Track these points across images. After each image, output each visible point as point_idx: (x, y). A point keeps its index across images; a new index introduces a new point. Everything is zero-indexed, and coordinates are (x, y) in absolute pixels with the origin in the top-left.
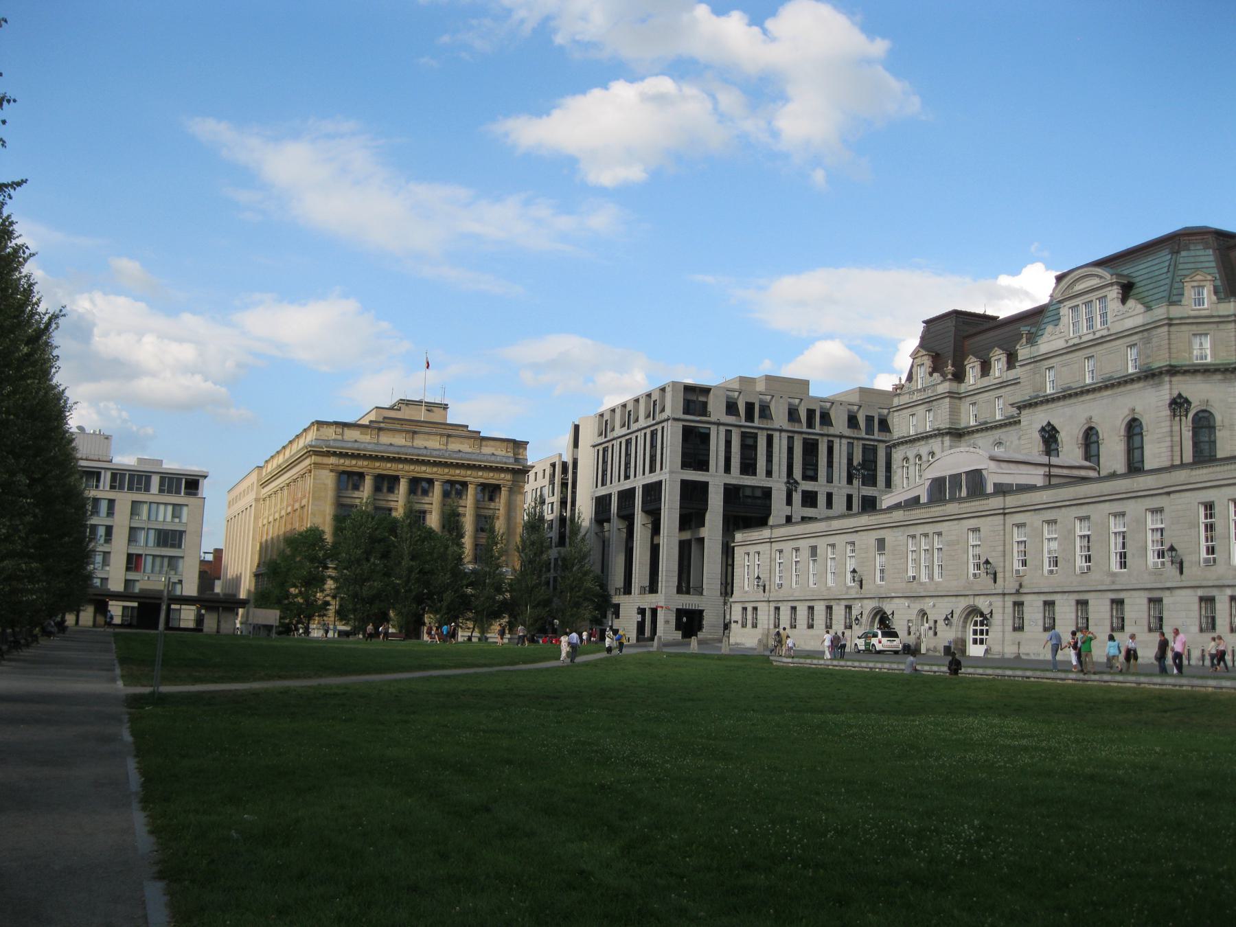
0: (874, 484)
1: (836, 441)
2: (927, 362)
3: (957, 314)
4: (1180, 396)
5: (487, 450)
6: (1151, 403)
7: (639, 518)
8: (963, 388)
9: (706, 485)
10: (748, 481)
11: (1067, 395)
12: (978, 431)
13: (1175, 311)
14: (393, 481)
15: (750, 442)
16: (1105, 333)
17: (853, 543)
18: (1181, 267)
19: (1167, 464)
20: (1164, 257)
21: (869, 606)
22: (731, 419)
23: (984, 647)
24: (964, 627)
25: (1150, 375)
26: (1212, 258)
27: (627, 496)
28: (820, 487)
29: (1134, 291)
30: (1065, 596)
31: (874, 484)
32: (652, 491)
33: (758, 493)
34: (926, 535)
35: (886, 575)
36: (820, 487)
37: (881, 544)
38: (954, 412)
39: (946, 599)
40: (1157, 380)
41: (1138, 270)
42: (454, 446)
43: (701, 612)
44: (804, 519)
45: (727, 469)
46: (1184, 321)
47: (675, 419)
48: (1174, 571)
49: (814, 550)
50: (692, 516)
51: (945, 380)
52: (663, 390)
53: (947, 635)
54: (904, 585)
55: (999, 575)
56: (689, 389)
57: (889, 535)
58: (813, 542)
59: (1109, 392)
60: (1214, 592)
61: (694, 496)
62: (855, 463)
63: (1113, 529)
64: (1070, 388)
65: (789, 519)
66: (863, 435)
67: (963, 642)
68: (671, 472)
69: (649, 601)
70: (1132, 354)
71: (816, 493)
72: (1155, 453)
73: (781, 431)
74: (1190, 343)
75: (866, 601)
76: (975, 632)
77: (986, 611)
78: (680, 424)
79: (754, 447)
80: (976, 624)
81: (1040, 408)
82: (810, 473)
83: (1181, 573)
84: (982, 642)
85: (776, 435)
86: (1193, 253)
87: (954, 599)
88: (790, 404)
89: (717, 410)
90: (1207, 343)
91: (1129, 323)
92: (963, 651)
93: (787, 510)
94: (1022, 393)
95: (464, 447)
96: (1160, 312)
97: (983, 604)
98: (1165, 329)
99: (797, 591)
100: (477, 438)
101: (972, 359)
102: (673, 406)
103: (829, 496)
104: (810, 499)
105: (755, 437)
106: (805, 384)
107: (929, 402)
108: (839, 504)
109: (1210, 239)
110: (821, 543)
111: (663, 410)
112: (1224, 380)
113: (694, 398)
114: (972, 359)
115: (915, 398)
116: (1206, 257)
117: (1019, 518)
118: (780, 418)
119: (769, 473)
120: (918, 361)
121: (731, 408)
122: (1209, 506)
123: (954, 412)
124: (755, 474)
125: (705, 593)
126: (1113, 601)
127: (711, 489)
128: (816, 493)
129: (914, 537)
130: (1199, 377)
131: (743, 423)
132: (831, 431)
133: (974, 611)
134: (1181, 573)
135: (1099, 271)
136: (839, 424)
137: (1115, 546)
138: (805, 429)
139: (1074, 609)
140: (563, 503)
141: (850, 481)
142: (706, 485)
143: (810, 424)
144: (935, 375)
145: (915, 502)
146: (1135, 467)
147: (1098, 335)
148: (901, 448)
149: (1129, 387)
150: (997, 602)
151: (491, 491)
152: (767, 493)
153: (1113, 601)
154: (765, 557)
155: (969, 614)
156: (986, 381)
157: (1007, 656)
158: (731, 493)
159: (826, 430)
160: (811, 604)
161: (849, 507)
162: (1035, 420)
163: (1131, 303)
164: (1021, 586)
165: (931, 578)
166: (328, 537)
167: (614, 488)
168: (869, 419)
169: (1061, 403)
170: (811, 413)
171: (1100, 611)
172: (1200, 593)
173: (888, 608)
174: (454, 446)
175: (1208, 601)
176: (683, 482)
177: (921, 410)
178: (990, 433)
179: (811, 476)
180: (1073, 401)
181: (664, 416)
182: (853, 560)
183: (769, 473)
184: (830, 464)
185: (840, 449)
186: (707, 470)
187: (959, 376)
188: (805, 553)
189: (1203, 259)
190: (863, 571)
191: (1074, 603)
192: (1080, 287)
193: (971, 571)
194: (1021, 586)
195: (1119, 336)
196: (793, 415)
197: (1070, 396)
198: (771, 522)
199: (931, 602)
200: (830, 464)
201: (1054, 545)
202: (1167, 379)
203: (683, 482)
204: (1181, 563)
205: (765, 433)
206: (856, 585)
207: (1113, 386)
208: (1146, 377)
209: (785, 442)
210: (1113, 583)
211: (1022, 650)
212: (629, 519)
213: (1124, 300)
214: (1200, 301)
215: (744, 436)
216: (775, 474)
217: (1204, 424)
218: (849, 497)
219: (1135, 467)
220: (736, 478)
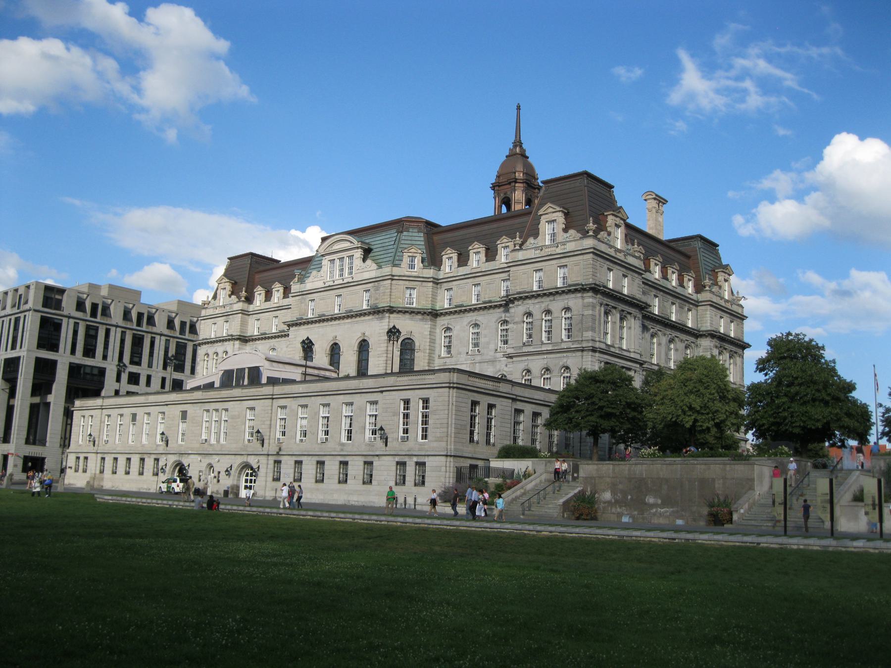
1: (158, 337)
2: (228, 287)
3: (253, 255)
4: (394, 327)
6: (375, 330)
8: (251, 308)
9: (54, 363)
10: (89, 362)
11: (322, 319)
12: (259, 339)
13: (396, 271)
15: (92, 332)
16: (350, 280)
17: (164, 413)
18: (403, 242)
19: (383, 372)
20: (393, 233)
21: (172, 459)
22: (79, 315)
23: (252, 491)
24: (239, 477)
25: (376, 311)
26: (422, 239)
28: (142, 370)
29: (371, 255)
30: (310, 458)
33: (96, 372)
34: (217, 410)
36: (142, 370)
37: (184, 415)
38: (244, 324)
39: (228, 457)
40: (381, 315)
41: (376, 241)
43: (44, 459)
44: (129, 393)
45: (73, 351)
46: (401, 278)
47: (35, 311)
48: (382, 445)
49: (134, 416)
51: (239, 301)
53: (227, 482)
54: (198, 445)
55: (266, 442)
56: (48, 289)
57: (190, 409)
58: (133, 410)
59: (349, 320)
60: (406, 459)
62: (170, 355)
63: (344, 414)
64: (324, 315)
65: (117, 393)
66: (178, 335)
67: (238, 487)
68: (28, 351)
70: (366, 296)
71: (139, 374)
72: (375, 365)
73: (117, 326)
74: (404, 293)
75: (170, 456)
76: (246, 481)
77: (255, 466)
78: (39, 315)
79: (95, 337)
80: (247, 475)
81: (303, 327)
82: (136, 360)
83: (386, 445)
84: (250, 488)
85: (113, 329)
86: (410, 234)
87: (233, 457)
88: (125, 307)
89: (68, 305)
90: (415, 293)
91: (367, 275)
92: (237, 494)
93: (116, 386)
96: (387, 270)
98: (389, 281)
101: (259, 288)
102: (34, 300)
103: (149, 378)
104: (134, 379)
105: (96, 329)
106: (138, 293)
108: (156, 384)
110: (140, 412)
111: (26, 302)
112: (422, 320)
113: (52, 296)
114: (259, 288)
115: (217, 312)
116: (418, 237)
117: (282, 402)
118: (116, 315)
119: (105, 357)
120: (222, 286)
121: (80, 306)
122: (407, 402)
123: (244, 324)
124: (94, 357)
125: (47, 444)
126: (318, 462)
128: (139, 374)
129: (208, 411)
130: (407, 316)
131: (88, 318)
132: (154, 330)
133: (247, 466)
134: (386, 445)
136: (161, 325)
138: (135, 327)
139: (315, 467)
141: (165, 368)
142: (54, 363)
143: (139, 323)
144: (233, 297)
145: (210, 386)
146: (362, 372)
147: (345, 281)
148: (204, 346)
149: (362, 318)
150: (263, 460)
152: (102, 372)
153: (318, 462)
154: (97, 420)
155: (243, 468)
156: (268, 305)
157: (267, 498)
158: (74, 369)
159: (150, 329)
160: (129, 456)
161: (163, 386)
162: (299, 334)
163: (369, 262)
164: (280, 449)
165: (218, 441)
168: (183, 324)
169: (317, 325)
170: (140, 315)
171: (309, 469)
172: (397, 459)
175: (402, 464)
176: (38, 361)
178: (267, 341)
180: (325, 324)
181: (27, 307)
182: (163, 425)
183: (105, 357)
185: (160, 343)
186: (57, 351)
187: (249, 300)
188: (128, 418)
189: (417, 238)
191: (315, 463)
192: (337, 247)
193: (247, 437)
194: (280, 449)
196: (127, 315)
197: (324, 320)
198: (103, 393)
199: (216, 458)
201: (305, 422)
202: (387, 315)
203: (38, 361)
204: (387, 439)
205: (105, 327)
206: (163, 444)
207: (352, 317)
208: (374, 313)
210: (342, 450)
211: (278, 495)
214: (412, 266)
215: (88, 328)
217: (408, 347)
218: (164, 379)
219: (362, 372)
220: (79, 358)
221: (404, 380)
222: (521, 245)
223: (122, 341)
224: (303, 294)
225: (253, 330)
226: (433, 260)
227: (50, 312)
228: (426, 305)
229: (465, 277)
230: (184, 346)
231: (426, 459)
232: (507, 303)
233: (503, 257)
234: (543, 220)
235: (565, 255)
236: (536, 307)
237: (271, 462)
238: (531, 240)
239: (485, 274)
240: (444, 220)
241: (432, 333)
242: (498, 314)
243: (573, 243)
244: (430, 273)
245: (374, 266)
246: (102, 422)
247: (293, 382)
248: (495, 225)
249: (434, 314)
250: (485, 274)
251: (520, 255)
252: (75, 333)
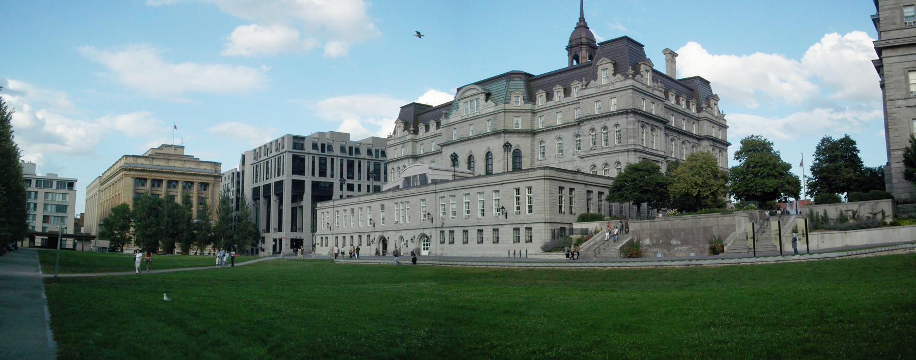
0: (379, 180)
2: (402, 125)
5: (203, 167)
6: (496, 145)
7: (273, 197)
8: (418, 137)
9: (303, 181)
10: (323, 179)
11: (462, 141)
13: (508, 107)
14: (160, 182)
20: (503, 82)
21: (378, 235)
22: (315, 152)
25: (496, 133)
27: (267, 187)
28: (355, 182)
31: (379, 180)
32: (279, 185)
36: (355, 182)
37: (383, 207)
41: (493, 88)
42: (188, 165)
45: (313, 174)
50: (297, 195)
52: (283, 138)
53: (412, 247)
56: (295, 138)
57: (386, 203)
58: (352, 207)
61: (298, 186)
69: (278, 235)
72: (497, 167)
79: (325, 164)
85: (335, 159)
89: (308, 147)
90: (519, 120)
91: (488, 111)
92: (419, 254)
93: (341, 192)
94: (443, 140)
95: (192, 166)
96: (501, 106)
97: (427, 232)
99: (345, 228)
100: (198, 161)
101: (421, 124)
102: (288, 146)
103: (359, 186)
104: (351, 187)
105: (325, 159)
106: (348, 135)
107: (403, 143)
108: (364, 189)
109: (523, 77)
110: (356, 207)
113: (298, 142)
114: (421, 124)
116: (520, 84)
118: (337, 151)
119: (332, 176)
121: (315, 146)
123: (414, 148)
126: (478, 230)
130: (516, 135)
132: (360, 156)
135: (477, 87)
136: (364, 154)
140: (238, 191)
141: (368, 179)
142: (303, 181)
143: (350, 153)
145: (397, 188)
146: (489, 173)
150: (433, 231)
151: (205, 186)
152: (331, 185)
153: (478, 230)
154: (331, 214)
156: (428, 134)
158: (315, 185)
159: (358, 156)
162: (448, 151)
163: (489, 102)
165: (405, 221)
166: (131, 208)
167: (261, 184)
168: (377, 151)
170: (351, 148)
173: (386, 235)
174: (188, 165)
177: (399, 147)
179: (351, 177)
181: (284, 150)
183: (332, 176)
184: (359, 171)
187: (416, 132)
188: (349, 212)
190: (375, 220)
196: (342, 149)
198: (334, 198)
199: (405, 232)
200: (359, 171)
211: (445, 252)
212: (268, 198)
213: (486, 101)
214: (517, 102)
215: (320, 159)
217: (517, 155)
218: (368, 186)
220: (317, 178)
221: (516, 176)
222: (586, 85)
223: (342, 165)
224: (449, 125)
225: (420, 151)
226: (530, 97)
227: (297, 152)
228: (528, 127)
229: (551, 108)
230: (379, 164)
232: (580, 122)
233: (575, 93)
234: (600, 68)
236: (597, 125)
237: (438, 232)
238: (593, 82)
239: (564, 105)
240: (536, 72)
241: (532, 145)
242: (573, 131)
244: (529, 106)
245: (493, 104)
247: (447, 181)
248: (570, 73)
249: (533, 133)
250: (564, 105)
251: (587, 92)
252: (313, 162)
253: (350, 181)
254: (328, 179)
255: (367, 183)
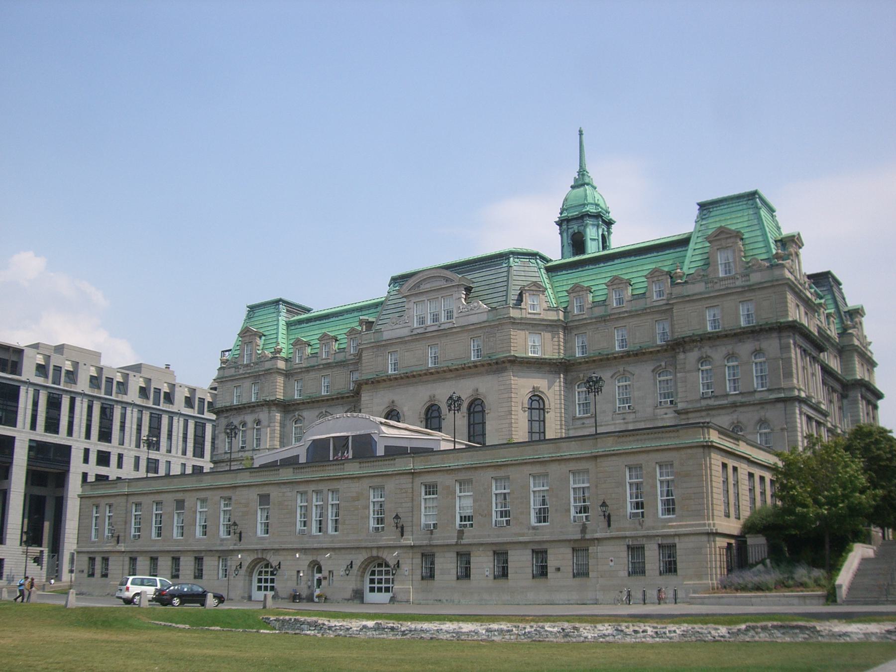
9: (12, 440)
10: (51, 438)
22: (40, 380)
24: (362, 576)
35: (340, 527)
37: (264, 499)
45: (33, 426)
48: (603, 524)
84: (387, 590)
93: (85, 468)
103: (120, 457)
119: (70, 432)
121: (41, 369)
124: (57, 432)
127: (17, 444)
135: (448, 273)
137: (534, 505)
142: (12, 440)
145: (291, 462)
152: (66, 451)
158: (38, 449)
177: (247, 384)
179: (105, 436)
183: (70, 432)
185: (132, 416)
186: (15, 426)
190: (405, 520)
195: (464, 329)
209: (85, 405)
216: (75, 434)
231: (676, 540)
235: (751, 289)
243: (759, 274)
246: (128, 512)
252: (35, 404)
253: (104, 447)
254: (61, 438)
255: (134, 453)
